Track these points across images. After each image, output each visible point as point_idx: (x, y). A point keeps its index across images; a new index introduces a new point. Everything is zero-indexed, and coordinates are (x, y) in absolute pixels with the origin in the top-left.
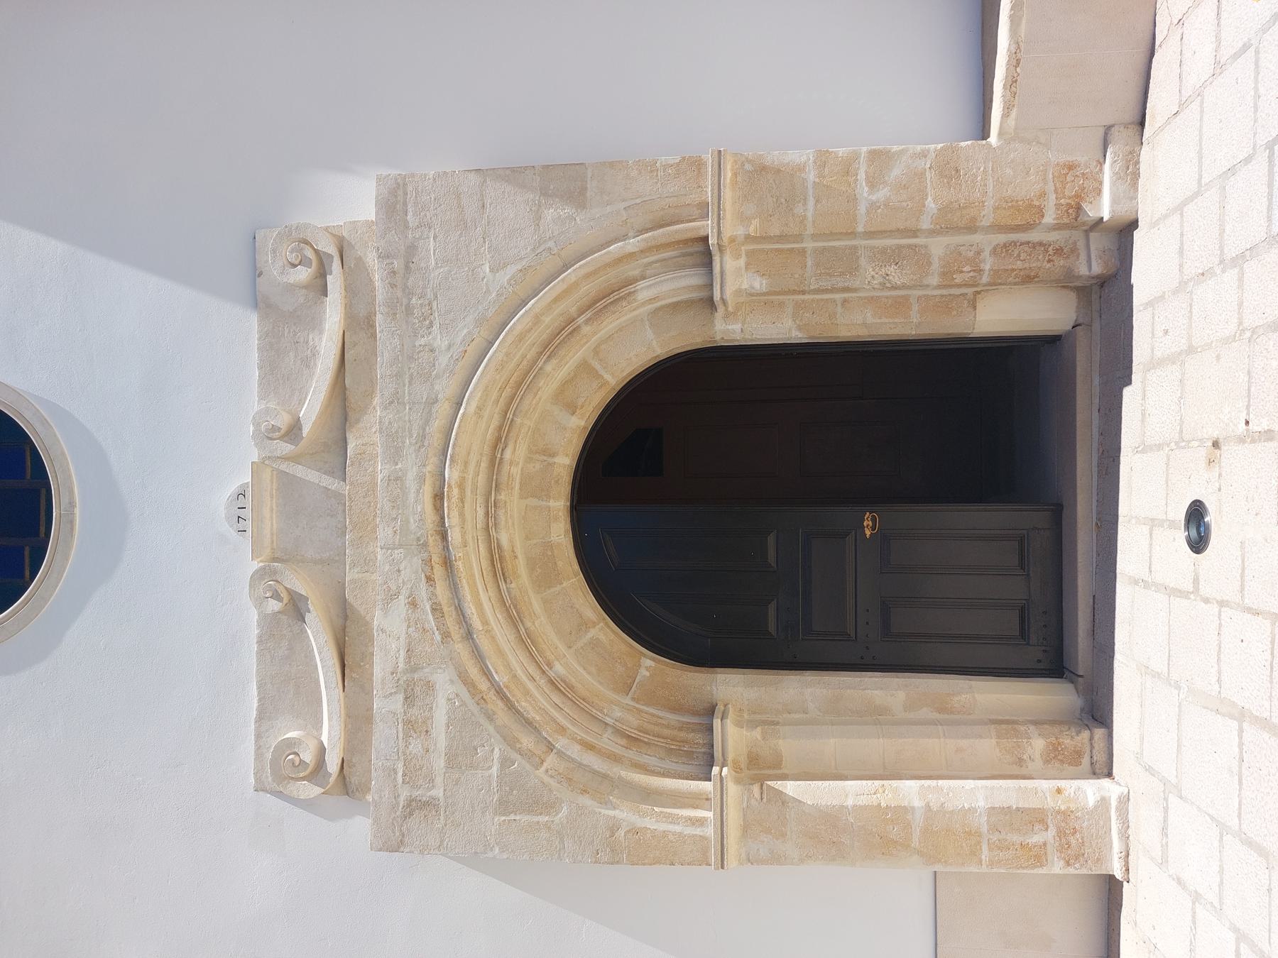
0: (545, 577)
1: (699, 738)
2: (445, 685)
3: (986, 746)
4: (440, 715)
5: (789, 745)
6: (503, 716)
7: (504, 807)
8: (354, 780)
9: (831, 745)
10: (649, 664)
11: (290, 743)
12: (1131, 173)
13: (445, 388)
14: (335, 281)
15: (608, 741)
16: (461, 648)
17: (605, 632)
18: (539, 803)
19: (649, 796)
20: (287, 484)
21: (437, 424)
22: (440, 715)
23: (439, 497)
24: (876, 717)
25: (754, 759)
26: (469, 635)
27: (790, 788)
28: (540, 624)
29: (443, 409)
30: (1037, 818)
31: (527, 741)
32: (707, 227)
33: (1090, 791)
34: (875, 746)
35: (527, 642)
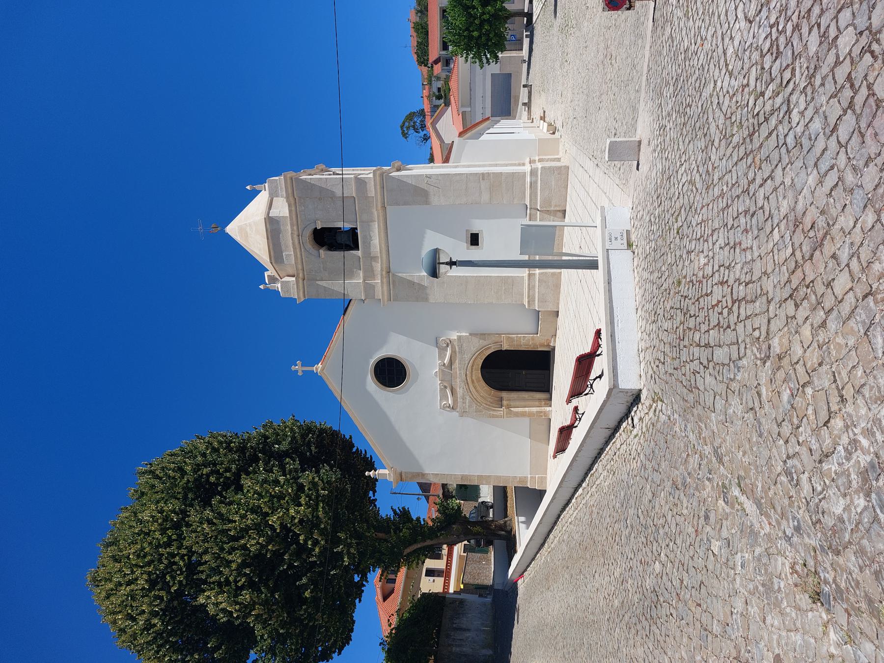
0: (478, 381)
1: (500, 402)
2: (468, 398)
3: (537, 403)
4: (467, 401)
5: (512, 404)
6: (475, 401)
7: (476, 412)
8: (454, 408)
9: (517, 403)
10: (493, 391)
11: (445, 404)
12: (555, 341)
13: (467, 362)
14: (450, 346)
15: (488, 403)
16: (470, 393)
17: (487, 388)
18: (480, 411)
19: (494, 410)
20: (443, 371)
21: (465, 367)
22: (467, 401)
23: (466, 375)
24: (524, 399)
25: (507, 405)
26: (471, 392)
27: (512, 409)
28: (478, 388)
29: (466, 365)
30: (542, 412)
31: (479, 404)
32: (502, 344)
33: (548, 409)
34: (523, 403)
35: (477, 391)
